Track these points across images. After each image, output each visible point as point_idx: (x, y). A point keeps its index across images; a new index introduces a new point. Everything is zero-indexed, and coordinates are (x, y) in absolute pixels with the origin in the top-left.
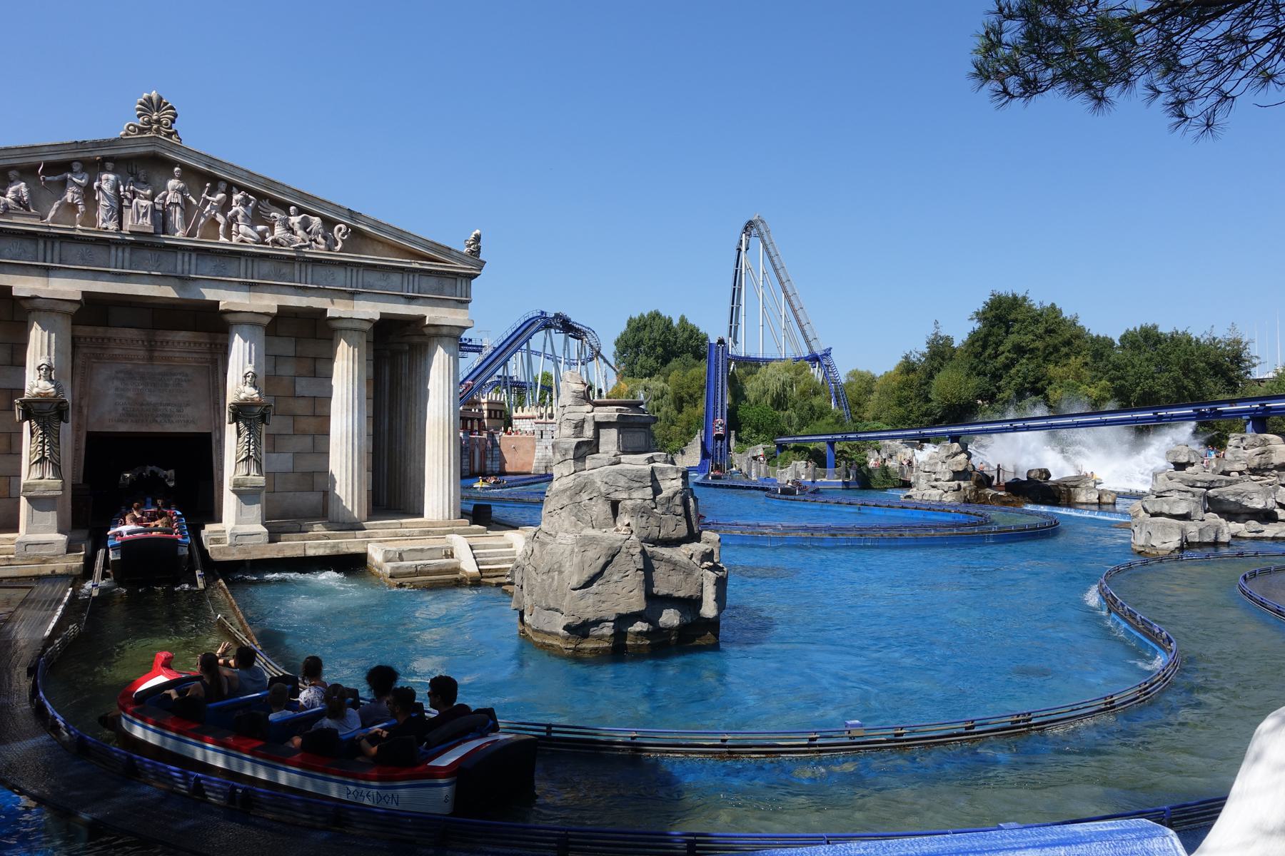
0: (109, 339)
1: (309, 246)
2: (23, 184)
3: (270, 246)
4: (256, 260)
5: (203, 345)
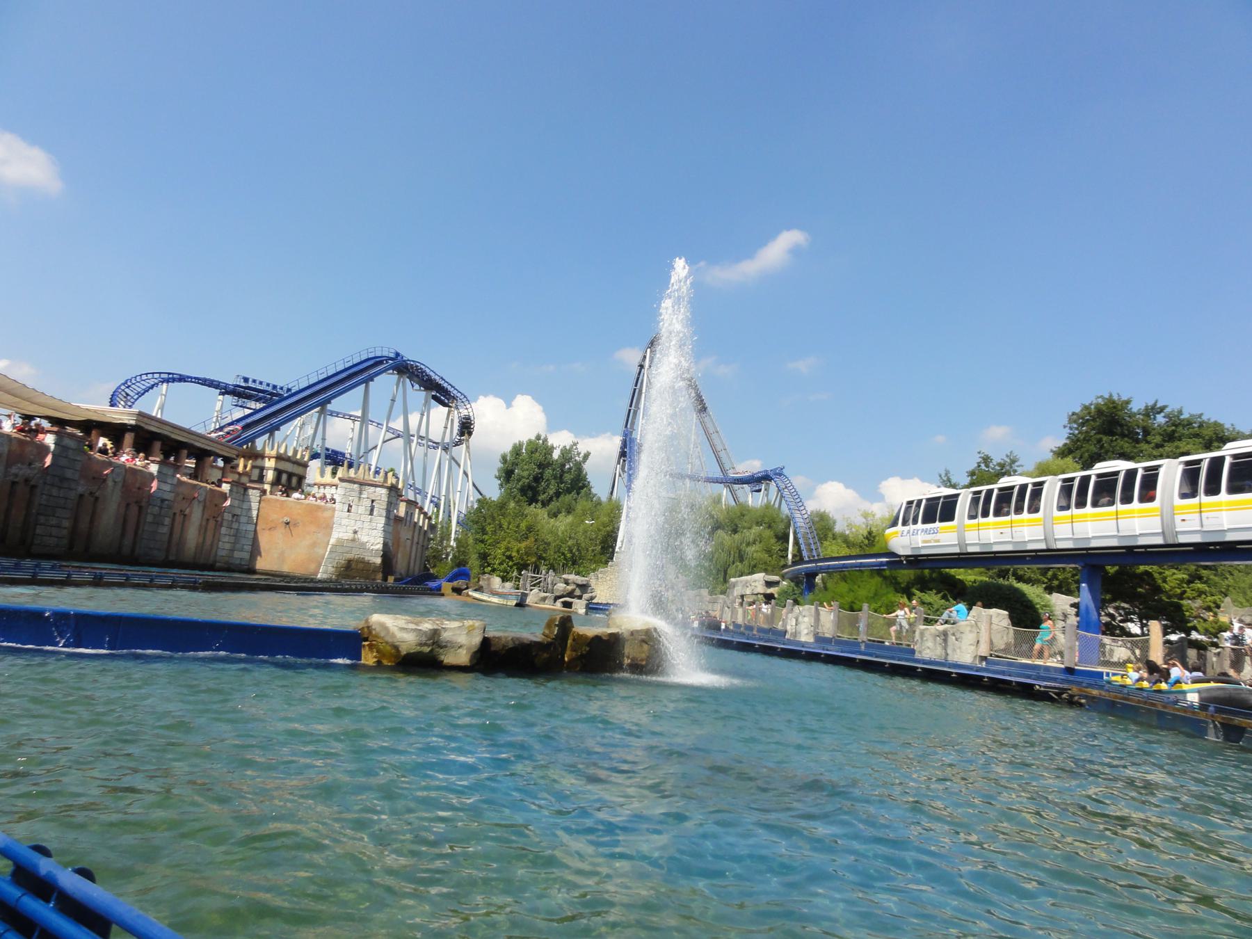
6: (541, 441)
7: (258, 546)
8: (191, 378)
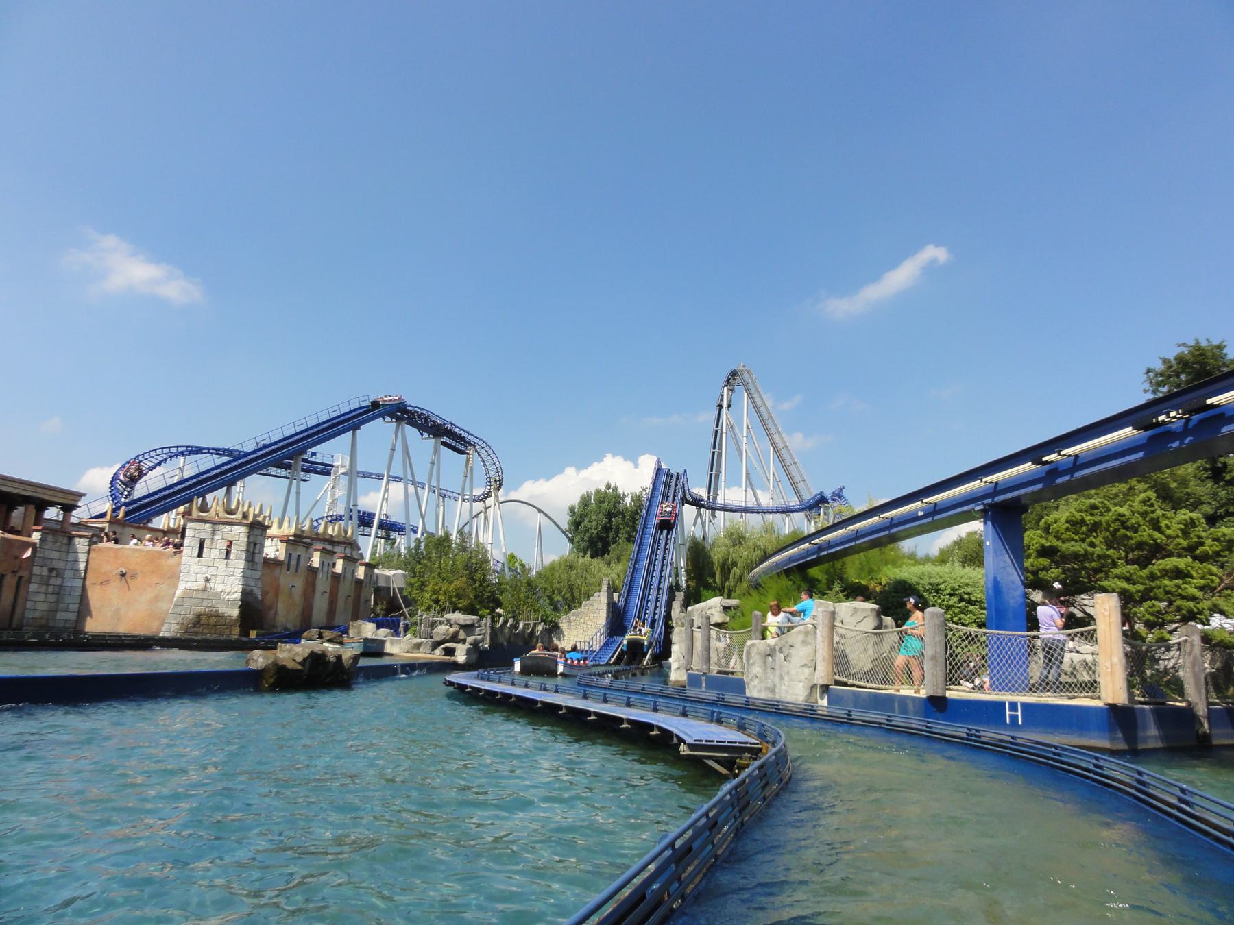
6: (611, 490)
7: (88, 605)
8: (209, 449)
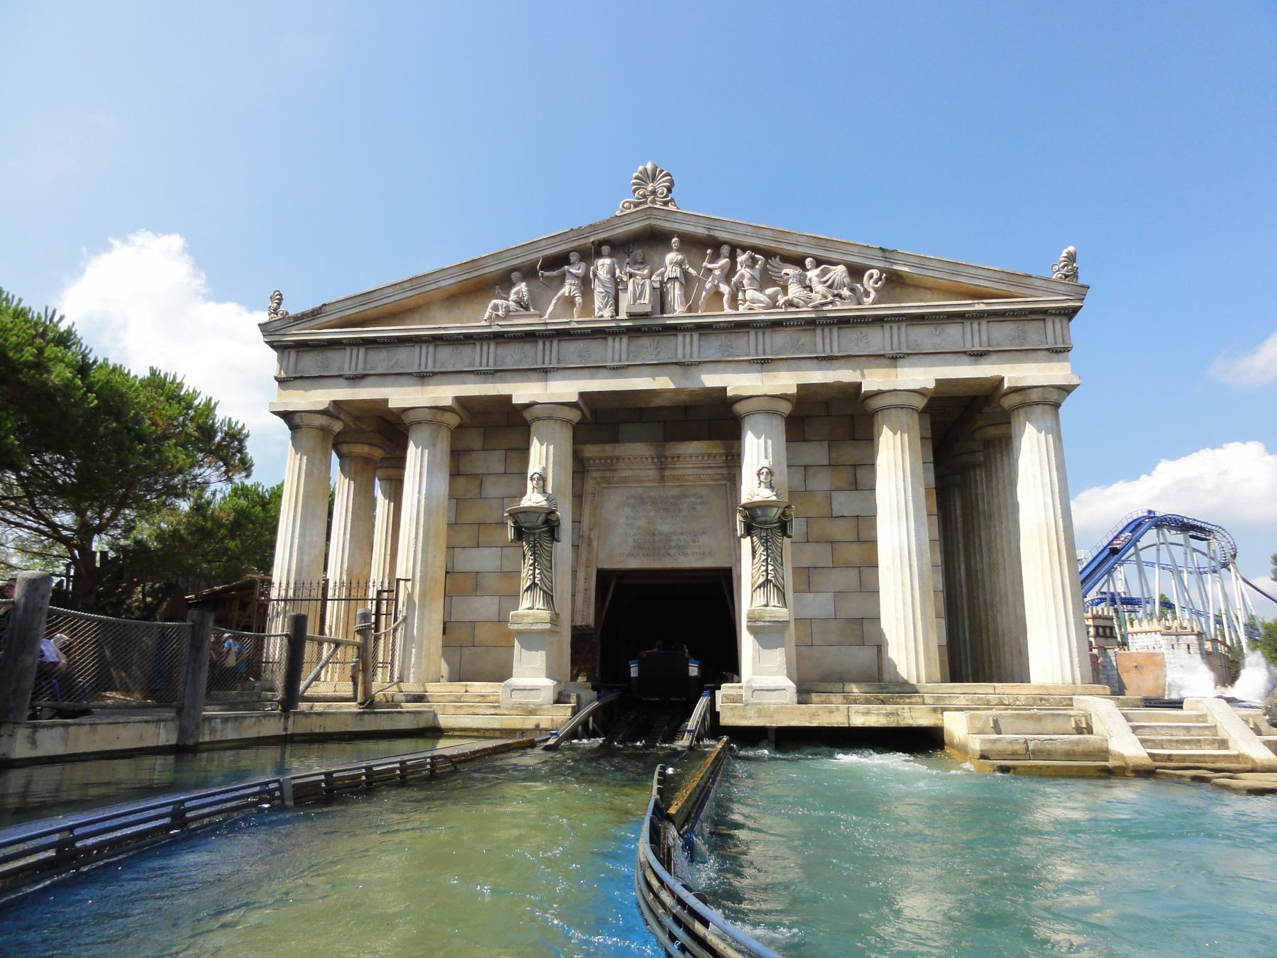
0: (618, 459)
1: (831, 303)
2: (524, 284)
3: (783, 310)
4: (768, 331)
5: (718, 458)
7: (1123, 682)
